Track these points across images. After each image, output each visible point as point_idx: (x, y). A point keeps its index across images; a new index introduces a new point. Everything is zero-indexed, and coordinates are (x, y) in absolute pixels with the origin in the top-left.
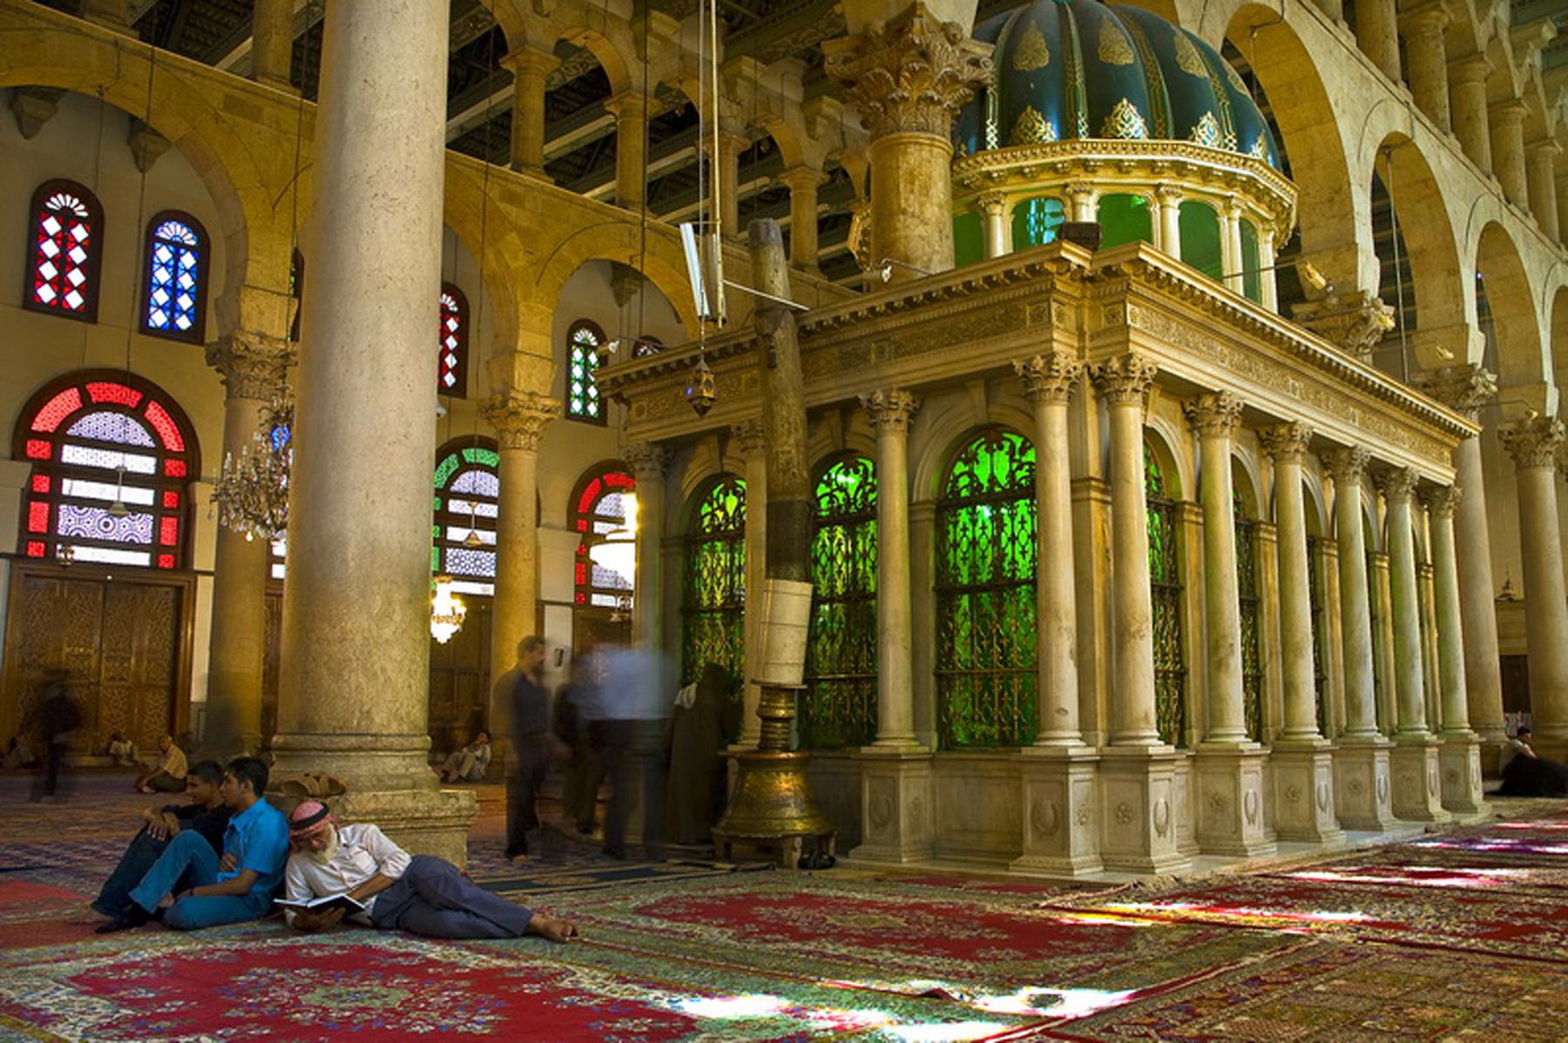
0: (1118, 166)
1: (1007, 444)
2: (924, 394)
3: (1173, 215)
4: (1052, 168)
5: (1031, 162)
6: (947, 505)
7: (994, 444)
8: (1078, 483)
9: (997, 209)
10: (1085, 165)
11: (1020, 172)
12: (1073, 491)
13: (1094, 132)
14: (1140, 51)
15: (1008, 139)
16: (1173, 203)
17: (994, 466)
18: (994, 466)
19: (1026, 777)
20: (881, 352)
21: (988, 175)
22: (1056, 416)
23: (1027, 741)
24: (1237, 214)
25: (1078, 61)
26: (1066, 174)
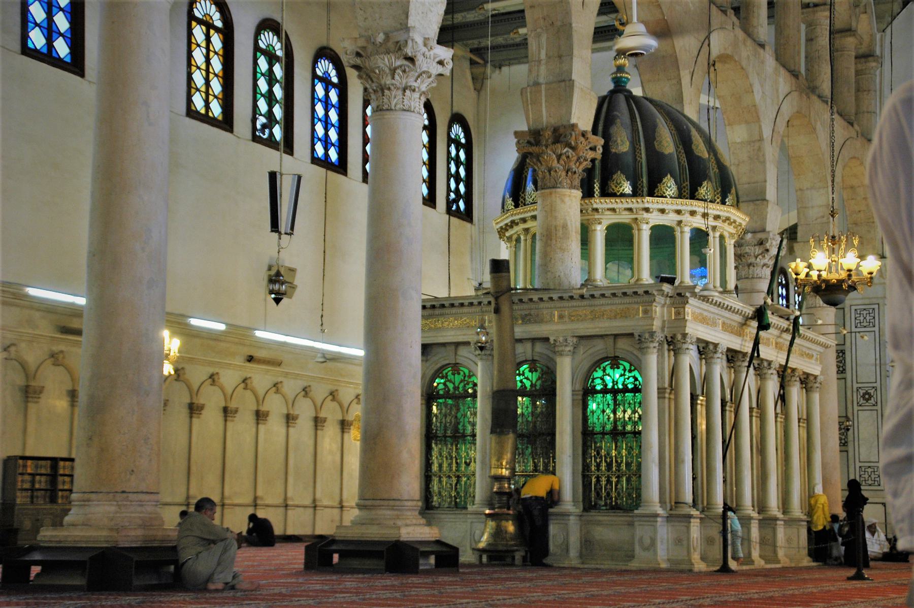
0: (662, 211)
1: (622, 367)
2: (581, 338)
3: (687, 236)
4: (630, 210)
5: (620, 206)
6: (588, 392)
7: (615, 365)
8: (661, 391)
9: (599, 227)
10: (647, 210)
11: (613, 210)
12: (658, 393)
13: (651, 194)
14: (677, 147)
15: (606, 193)
16: (687, 230)
17: (615, 377)
18: (615, 377)
19: (636, 523)
20: (561, 317)
21: (596, 210)
22: (652, 360)
23: (637, 506)
24: (717, 234)
25: (642, 144)
26: (637, 213)
